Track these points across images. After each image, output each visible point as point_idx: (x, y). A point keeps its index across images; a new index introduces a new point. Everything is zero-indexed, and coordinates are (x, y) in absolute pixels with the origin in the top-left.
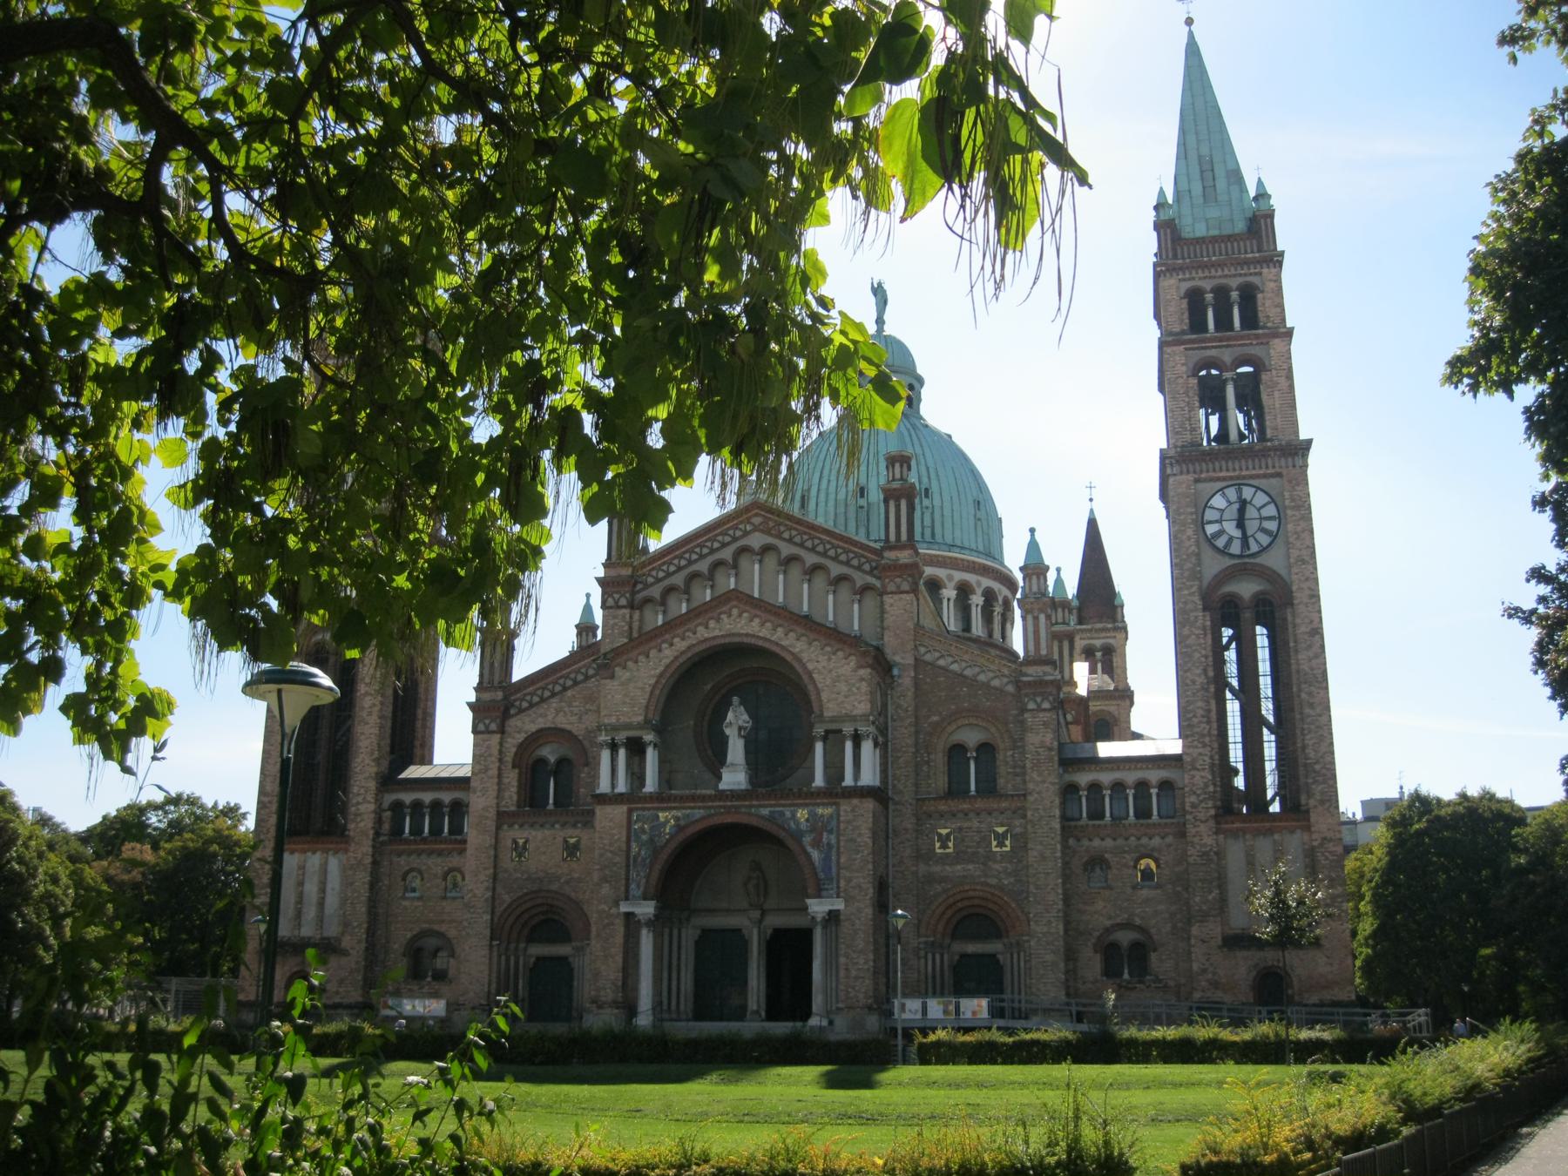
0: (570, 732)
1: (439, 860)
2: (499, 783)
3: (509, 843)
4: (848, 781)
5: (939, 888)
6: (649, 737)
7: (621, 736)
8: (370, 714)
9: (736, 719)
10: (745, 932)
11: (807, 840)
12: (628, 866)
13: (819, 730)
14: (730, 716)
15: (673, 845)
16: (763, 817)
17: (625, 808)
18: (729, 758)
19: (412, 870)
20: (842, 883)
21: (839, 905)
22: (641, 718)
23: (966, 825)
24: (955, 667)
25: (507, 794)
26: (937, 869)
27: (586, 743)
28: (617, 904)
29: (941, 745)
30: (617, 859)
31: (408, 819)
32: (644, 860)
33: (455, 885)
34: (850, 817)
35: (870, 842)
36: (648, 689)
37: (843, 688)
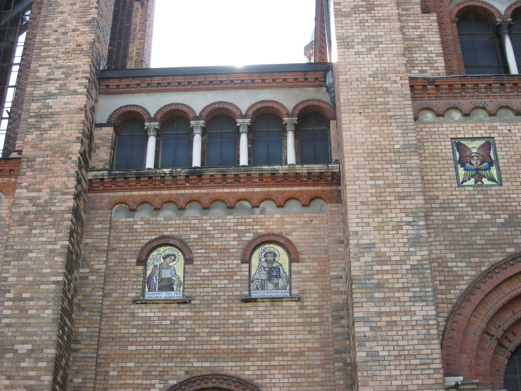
1: (231, 220)
3: (446, 148)
19: (163, 241)
25: (420, 57)
31: (152, 142)
33: (273, 273)
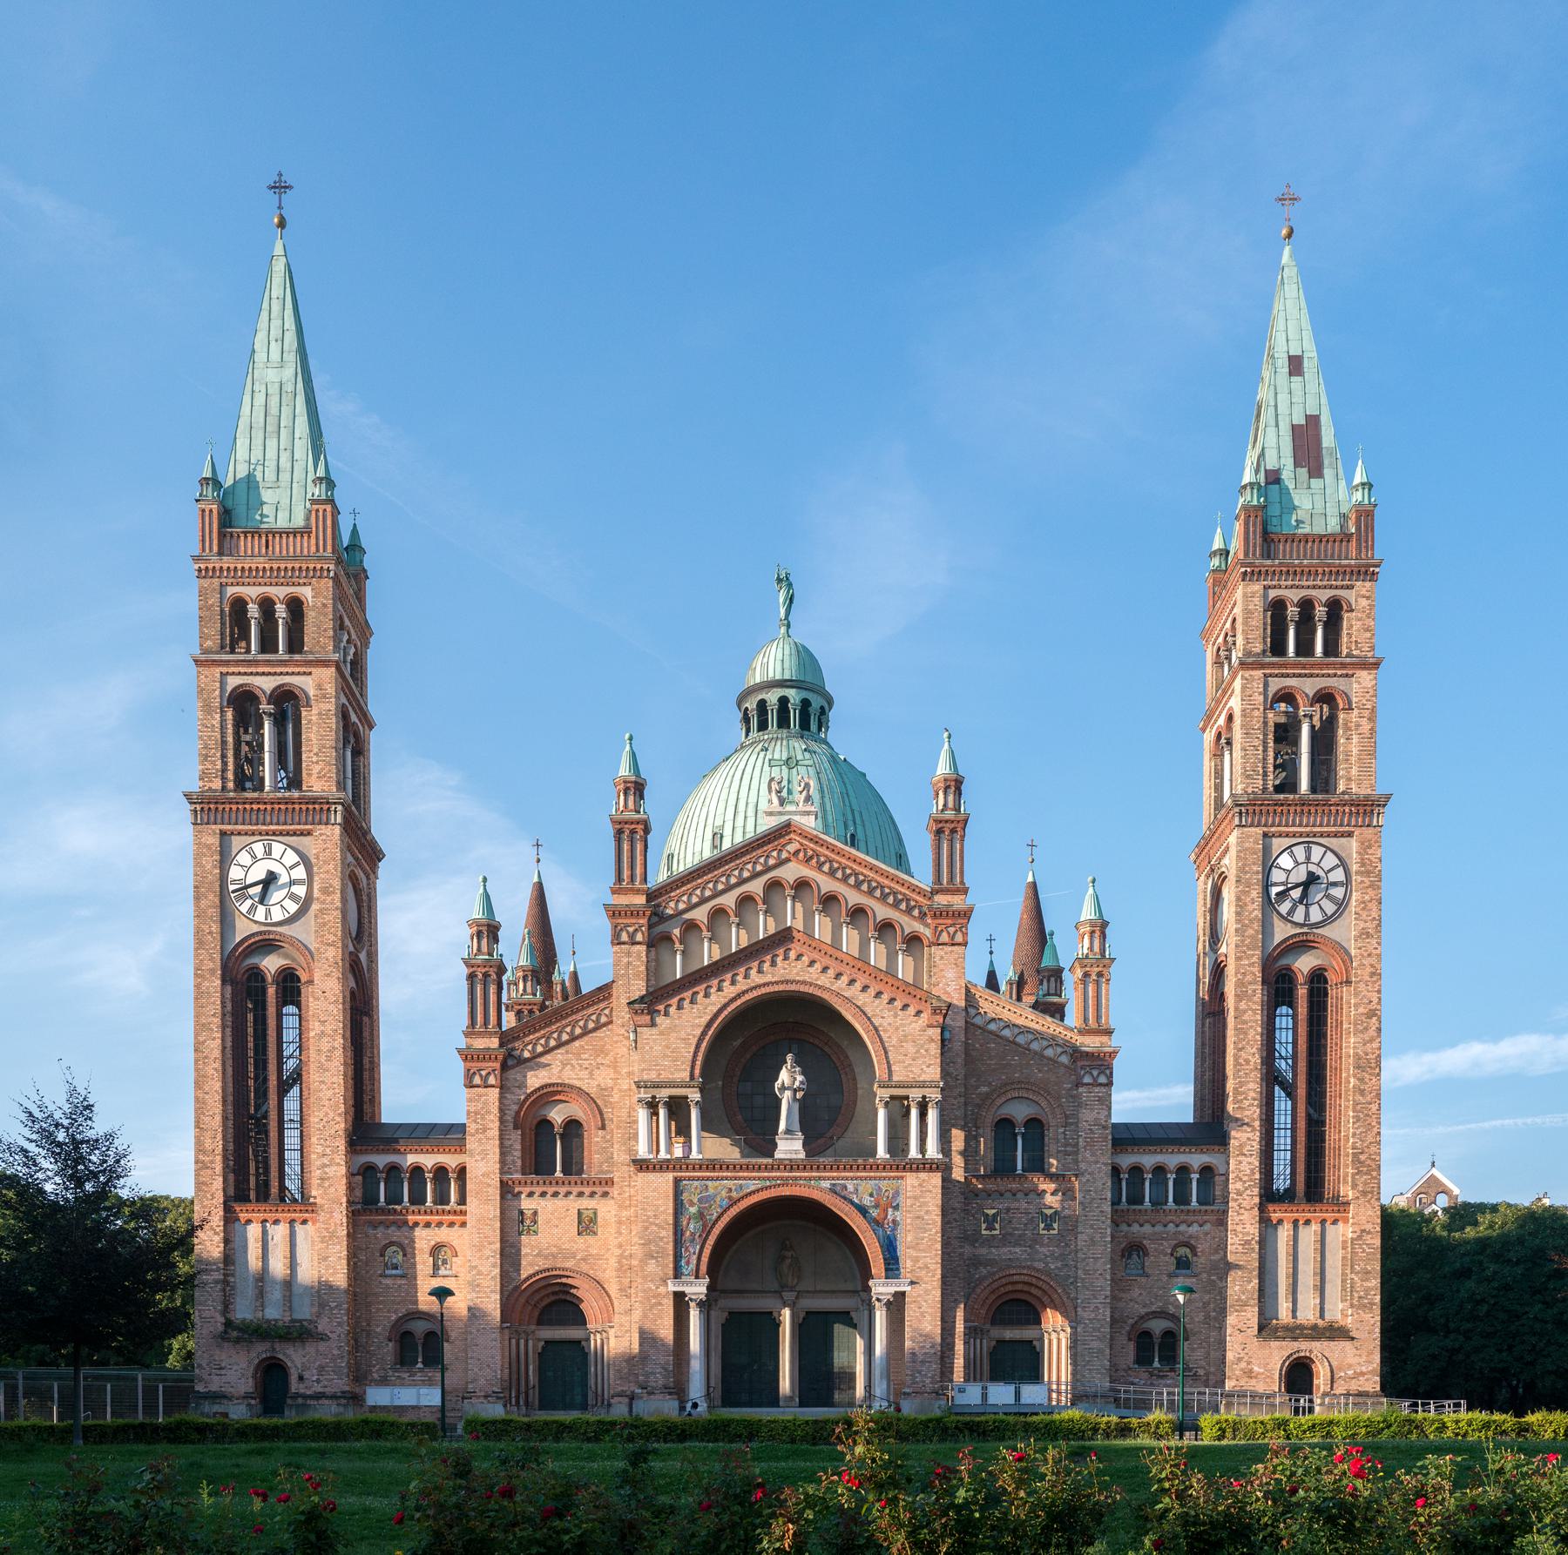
2: (502, 1146)
4: (914, 1153)
8: (329, 1059)
17: (670, 1176)
23: (1016, 1205)
28: (665, 1282)
29: (989, 1118)
30: (663, 1233)
32: (693, 1234)
35: (939, 1220)
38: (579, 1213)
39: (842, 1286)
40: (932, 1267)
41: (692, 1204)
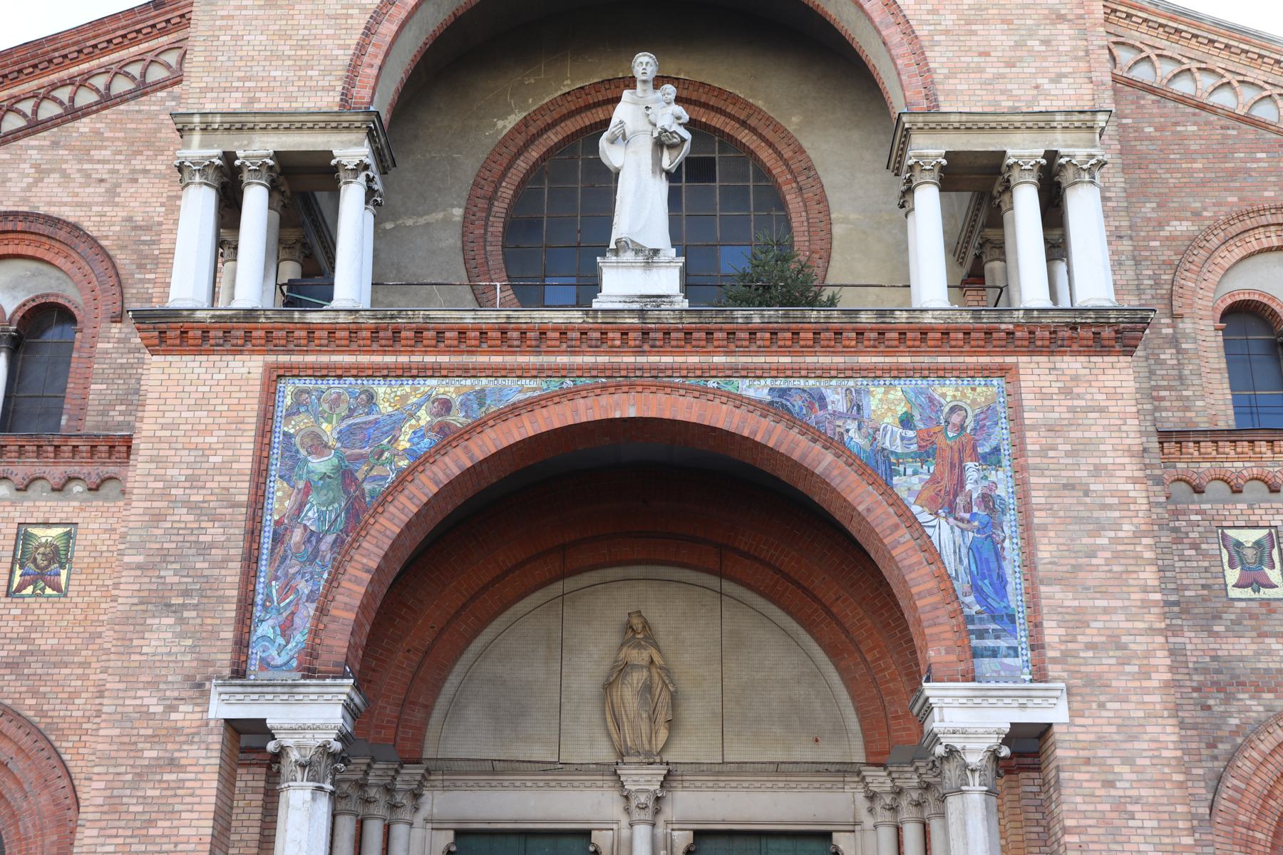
0: (75, 228)
5: (1255, 706)
6: (351, 150)
7: (258, 148)
9: (642, 126)
10: (601, 839)
11: (909, 483)
12: (251, 560)
13: (929, 148)
14: (625, 112)
15: (425, 487)
16: (754, 404)
18: (622, 227)
20: (1052, 633)
21: (1054, 712)
22: (330, 101)
24: (1224, 99)
26: (1241, 646)
27: (122, 258)
28: (199, 688)
30: (213, 533)
34: (1060, 410)
36: (360, 22)
37: (1000, 39)
38: (23, 536)
39: (805, 752)
40: (1138, 644)
41: (318, 445)
